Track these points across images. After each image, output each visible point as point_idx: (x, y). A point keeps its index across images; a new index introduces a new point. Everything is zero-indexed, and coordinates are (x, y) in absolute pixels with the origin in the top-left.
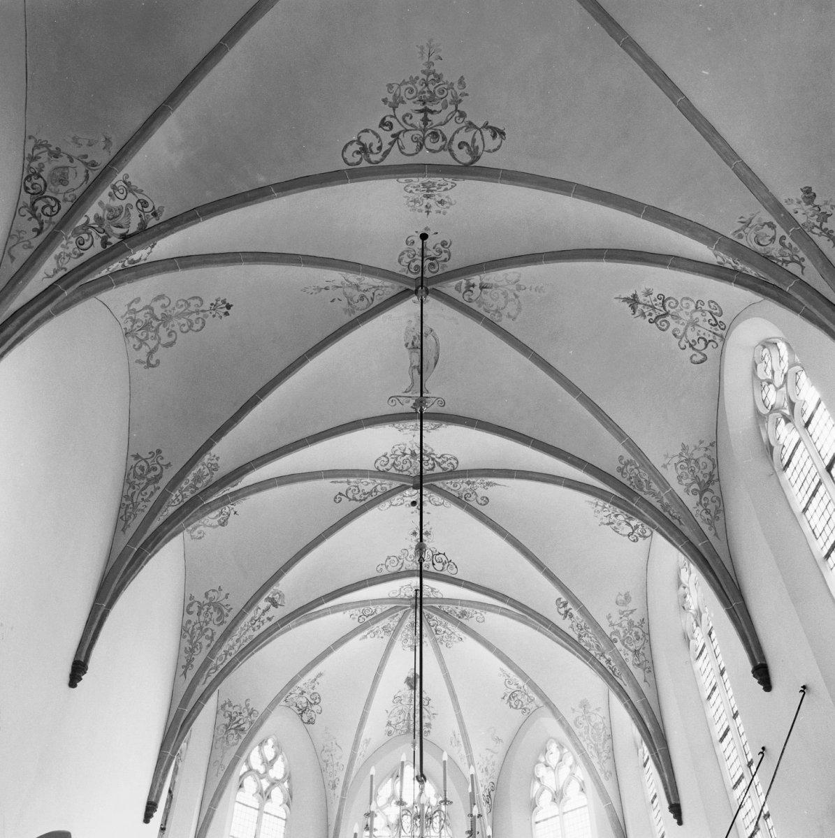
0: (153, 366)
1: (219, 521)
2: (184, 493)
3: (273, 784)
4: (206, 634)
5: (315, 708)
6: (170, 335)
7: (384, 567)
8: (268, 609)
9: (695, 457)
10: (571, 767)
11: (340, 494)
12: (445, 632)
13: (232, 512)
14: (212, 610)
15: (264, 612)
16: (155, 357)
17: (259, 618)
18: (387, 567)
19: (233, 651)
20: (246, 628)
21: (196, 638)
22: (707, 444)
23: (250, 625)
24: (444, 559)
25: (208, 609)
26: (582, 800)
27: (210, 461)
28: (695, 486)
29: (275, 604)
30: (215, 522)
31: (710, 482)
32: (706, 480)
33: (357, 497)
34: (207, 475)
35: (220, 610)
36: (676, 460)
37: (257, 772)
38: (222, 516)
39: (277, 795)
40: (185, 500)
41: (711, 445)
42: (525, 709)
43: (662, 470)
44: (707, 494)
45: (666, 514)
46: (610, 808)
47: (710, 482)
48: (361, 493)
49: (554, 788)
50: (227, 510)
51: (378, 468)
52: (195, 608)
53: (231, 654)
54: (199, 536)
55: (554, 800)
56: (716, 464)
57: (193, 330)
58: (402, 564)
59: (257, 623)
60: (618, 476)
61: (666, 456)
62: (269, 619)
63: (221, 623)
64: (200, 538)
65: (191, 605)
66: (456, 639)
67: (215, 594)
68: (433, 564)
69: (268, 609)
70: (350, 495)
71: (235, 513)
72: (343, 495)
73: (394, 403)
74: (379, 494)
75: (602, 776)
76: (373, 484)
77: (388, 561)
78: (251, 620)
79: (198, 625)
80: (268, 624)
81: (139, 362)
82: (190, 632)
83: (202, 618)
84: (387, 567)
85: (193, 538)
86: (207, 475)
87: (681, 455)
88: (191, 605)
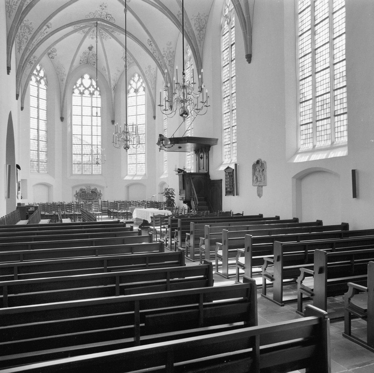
3: (41, 78)
5: (54, 53)
7: (88, 16)
9: (201, 19)
10: (141, 83)
12: (105, 35)
14: (26, 28)
15: (45, 30)
19: (35, 44)
22: (205, 15)
24: (111, 17)
26: (144, 93)
28: (199, 28)
29: (48, 27)
31: (203, 28)
32: (202, 27)
35: (29, 29)
36: (195, 18)
37: (36, 75)
39: (42, 81)
40: (28, 4)
41: (207, 16)
42: (129, 62)
43: (190, 20)
44: (201, 32)
45: (188, 34)
46: (152, 98)
47: (203, 28)
49: (135, 88)
53: (34, 45)
55: (135, 92)
56: (206, 23)
58: (95, 16)
59: (43, 34)
60: (177, 17)
61: (193, 15)
62: (47, 32)
63: (30, 34)
66: (109, 38)
67: (26, 22)
68: (106, 18)
75: (151, 89)
79: (21, 34)
80: (46, 34)
82: (18, 36)
83: (22, 31)
84: (89, 16)
87: (197, 16)
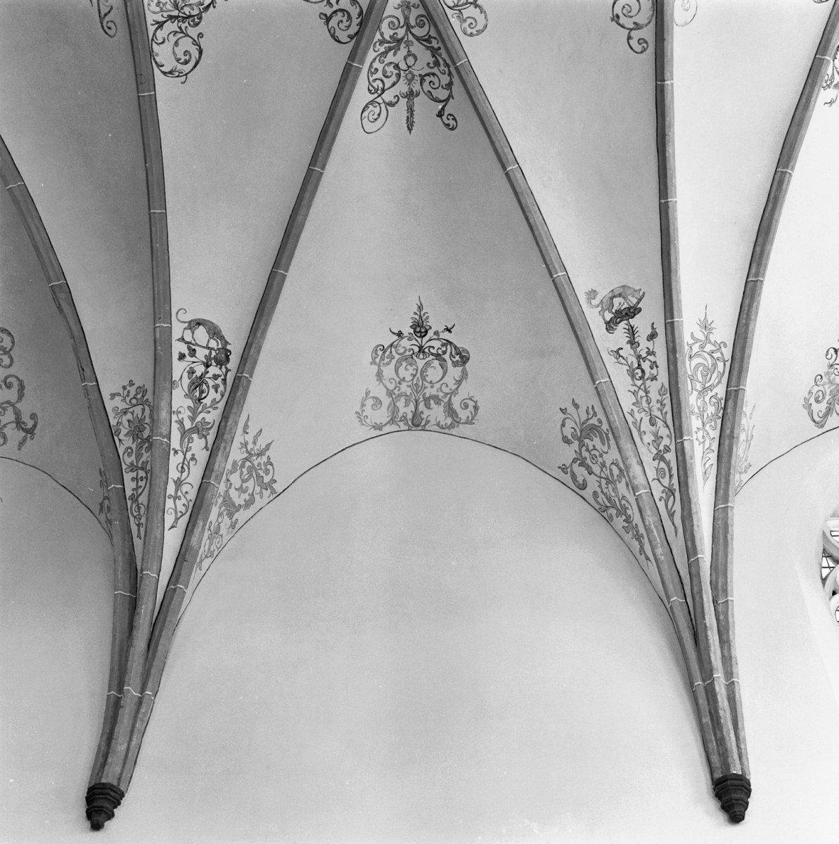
0: (35, 426)
1: (455, 364)
2: (140, 465)
4: (615, 478)
6: (9, 386)
8: (632, 331)
11: (440, 115)
13: (446, 335)
15: (633, 343)
16: (26, 418)
17: (639, 357)
18: (638, 26)
19: (666, 441)
20: (641, 393)
21: (616, 500)
23: (639, 383)
25: (587, 450)
27: (128, 399)
29: (632, 312)
30: (454, 372)
33: (445, 79)
34: (143, 410)
35: (593, 428)
38: (447, 357)
48: (435, 70)
50: (437, 344)
51: (351, 37)
52: (581, 472)
53: (667, 449)
54: (471, 408)
57: (11, 350)
59: (646, 366)
62: (652, 336)
64: (476, 408)
65: (574, 477)
67: (569, 424)
69: (632, 331)
70: (443, 94)
71: (449, 330)
72: (443, 108)
73: (110, 25)
74: (433, 33)
76: (408, 44)
77: (623, 20)
78: (633, 376)
79: (603, 481)
80: (660, 341)
81: (21, 444)
82: (608, 505)
83: (596, 469)
84: (638, 26)
85: (469, 422)
86: (143, 410)
88: (574, 477)
